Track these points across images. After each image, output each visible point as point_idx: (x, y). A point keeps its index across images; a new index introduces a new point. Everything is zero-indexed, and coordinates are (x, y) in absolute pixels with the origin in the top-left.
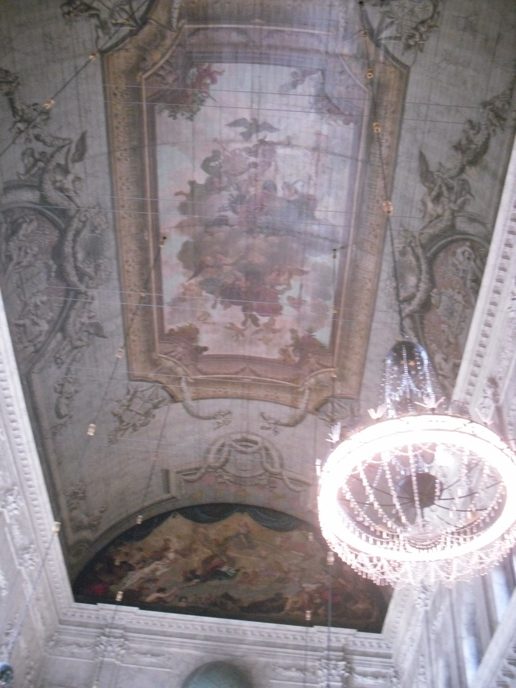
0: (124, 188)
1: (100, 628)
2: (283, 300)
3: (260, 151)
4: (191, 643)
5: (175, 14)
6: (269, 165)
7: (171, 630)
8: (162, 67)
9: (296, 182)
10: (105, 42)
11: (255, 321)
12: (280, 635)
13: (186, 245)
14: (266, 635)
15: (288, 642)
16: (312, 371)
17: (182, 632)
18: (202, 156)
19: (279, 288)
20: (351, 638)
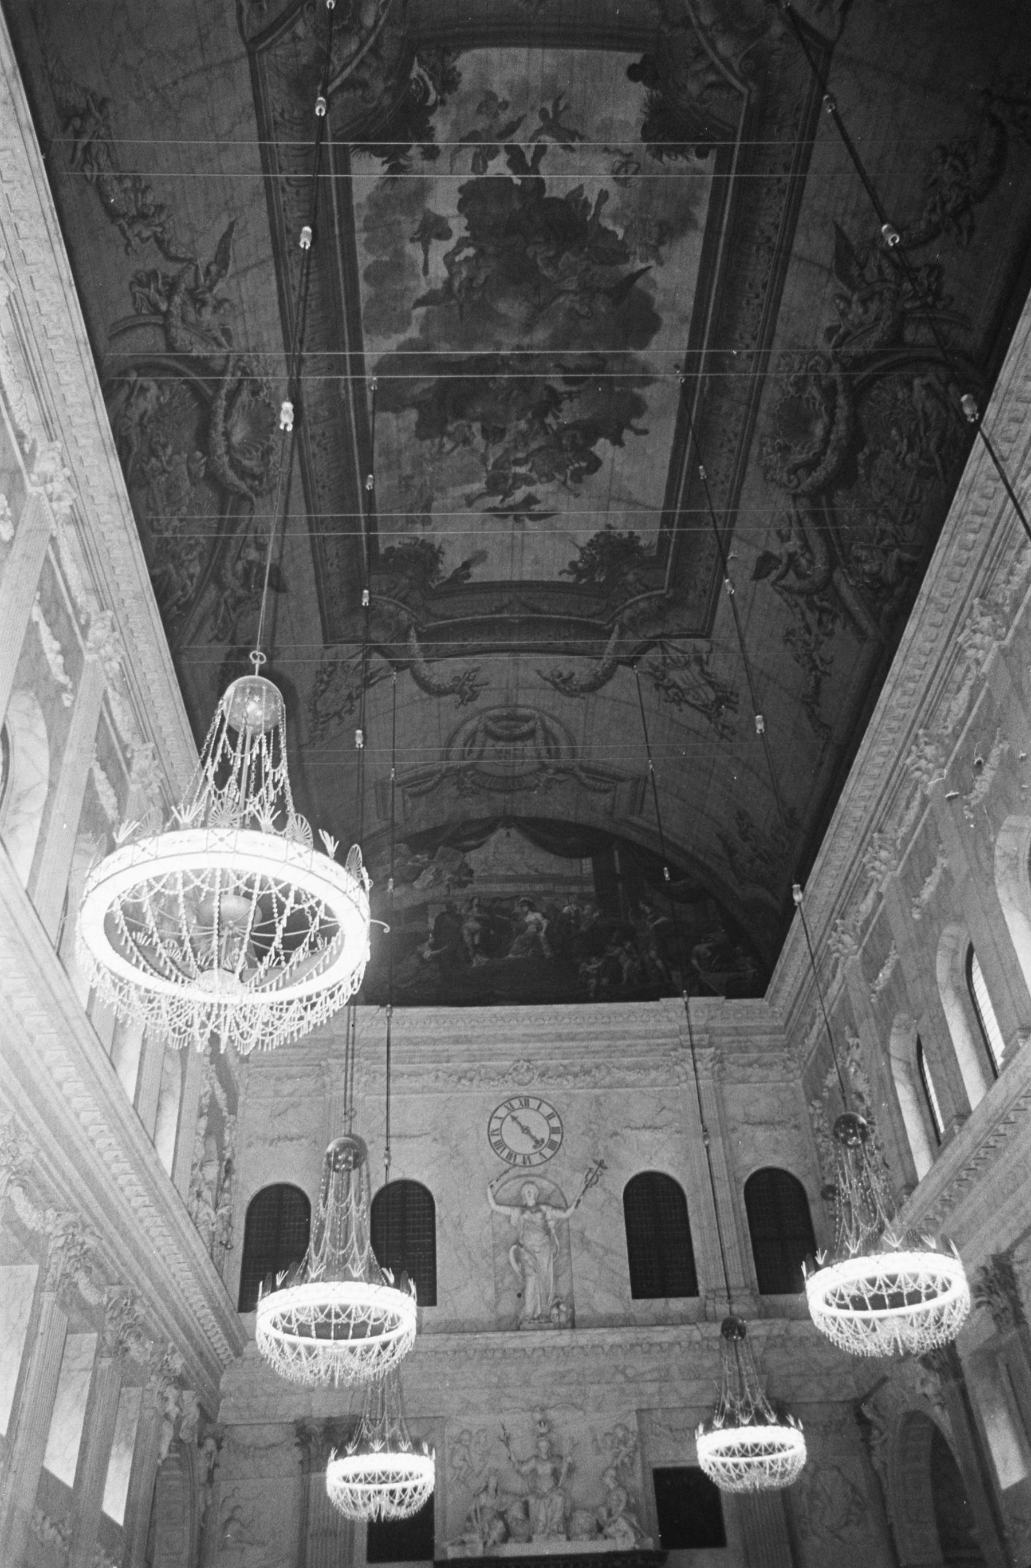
0: (721, 476)
2: (458, 226)
3: (510, 482)
5: (614, 635)
6: (494, 466)
8: (639, 593)
9: (452, 450)
10: (701, 644)
11: (516, 159)
13: (643, 345)
16: (374, 51)
18: (600, 477)
19: (470, 252)
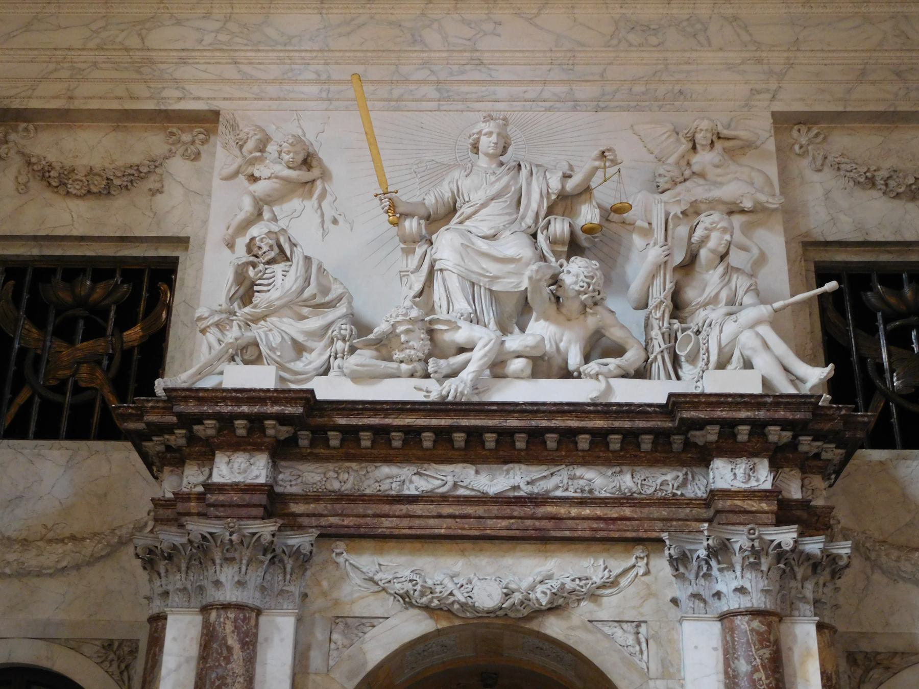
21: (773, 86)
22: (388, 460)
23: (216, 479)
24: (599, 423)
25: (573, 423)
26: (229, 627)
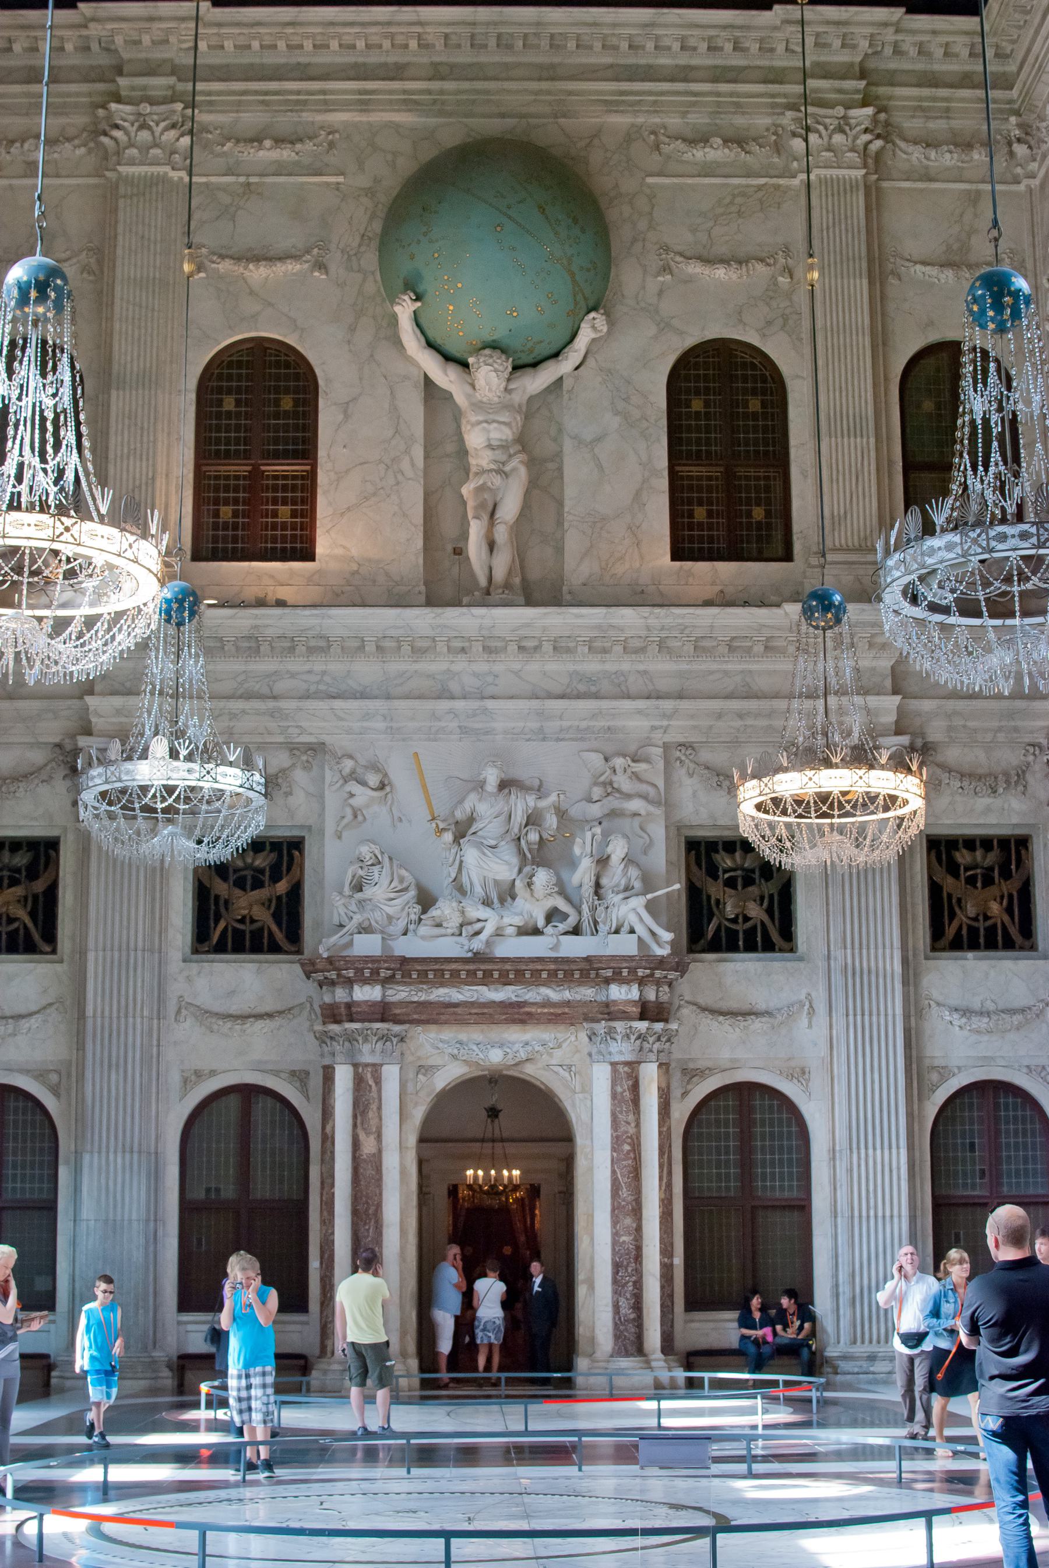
1: (101, 80)
4: (391, 92)
7: (323, 59)
12: (666, 42)
14: (624, 45)
15: (694, 62)
17: (361, 60)
20: (889, 35)
21: (665, 723)
22: (442, 985)
23: (355, 998)
24: (553, 967)
25: (540, 967)
26: (369, 1075)
